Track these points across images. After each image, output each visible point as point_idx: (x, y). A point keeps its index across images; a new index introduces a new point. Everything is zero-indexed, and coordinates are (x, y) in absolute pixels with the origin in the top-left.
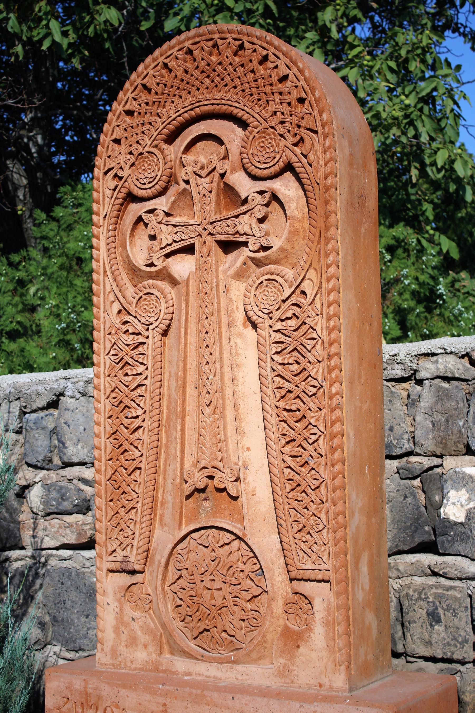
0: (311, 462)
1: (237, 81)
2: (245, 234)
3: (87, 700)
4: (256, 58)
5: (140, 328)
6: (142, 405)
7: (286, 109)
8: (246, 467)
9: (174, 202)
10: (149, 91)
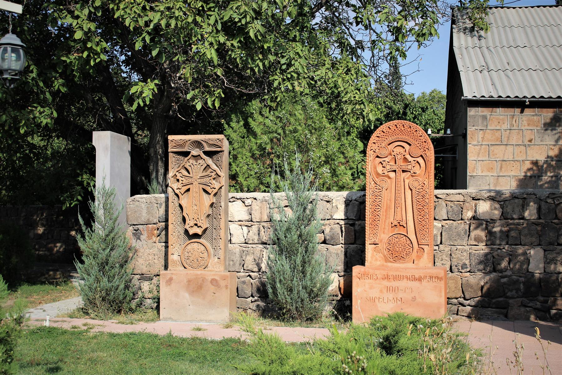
4: (414, 130)
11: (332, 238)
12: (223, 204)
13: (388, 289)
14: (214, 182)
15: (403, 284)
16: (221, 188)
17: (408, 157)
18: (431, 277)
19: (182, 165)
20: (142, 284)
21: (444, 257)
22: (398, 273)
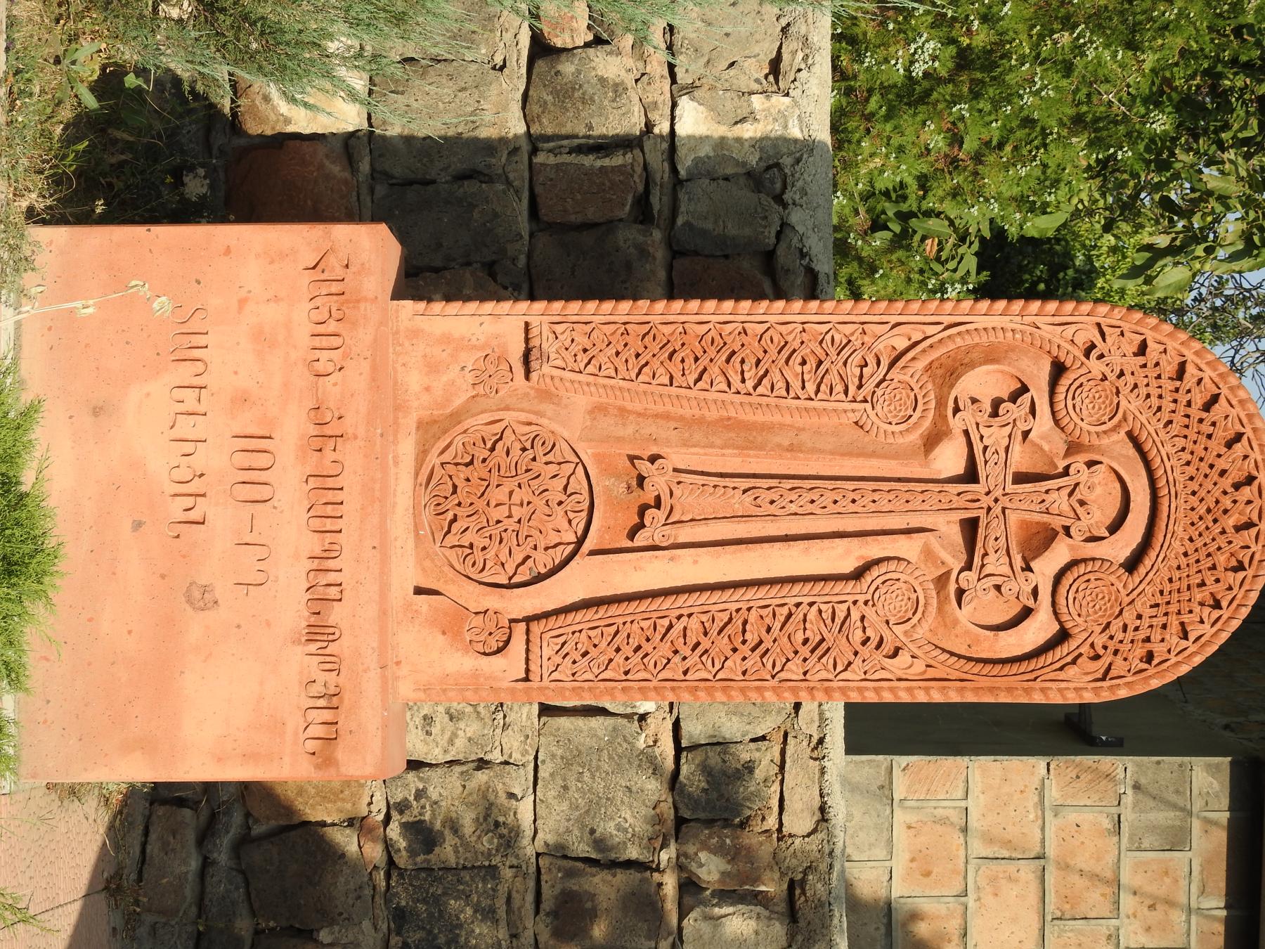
0: (677, 659)
1: (1192, 560)
2: (983, 566)
3: (347, 301)
4: (1219, 589)
5: (869, 386)
6: (760, 390)
7: (1141, 635)
8: (672, 559)
9: (1042, 449)
10: (1207, 407)
11: (567, 94)
13: (256, 442)
18: (332, 700)
21: (470, 728)
22: (352, 499)
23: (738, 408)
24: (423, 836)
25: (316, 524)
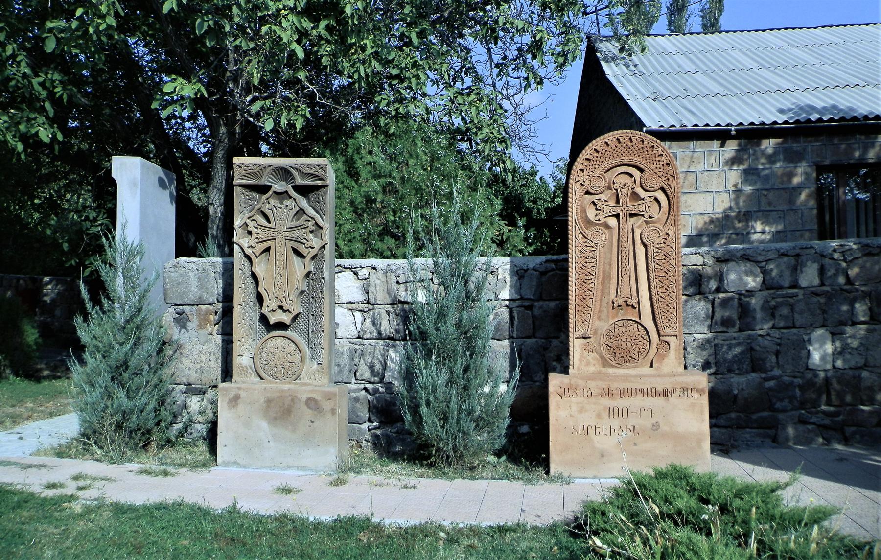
5: (593, 244)
12: (326, 274)
13: (610, 412)
14: (311, 236)
15: (638, 402)
16: (323, 247)
17: (639, 190)
19: (256, 208)
20: (188, 400)
23: (598, 281)
24: (706, 366)
25: (634, 395)
